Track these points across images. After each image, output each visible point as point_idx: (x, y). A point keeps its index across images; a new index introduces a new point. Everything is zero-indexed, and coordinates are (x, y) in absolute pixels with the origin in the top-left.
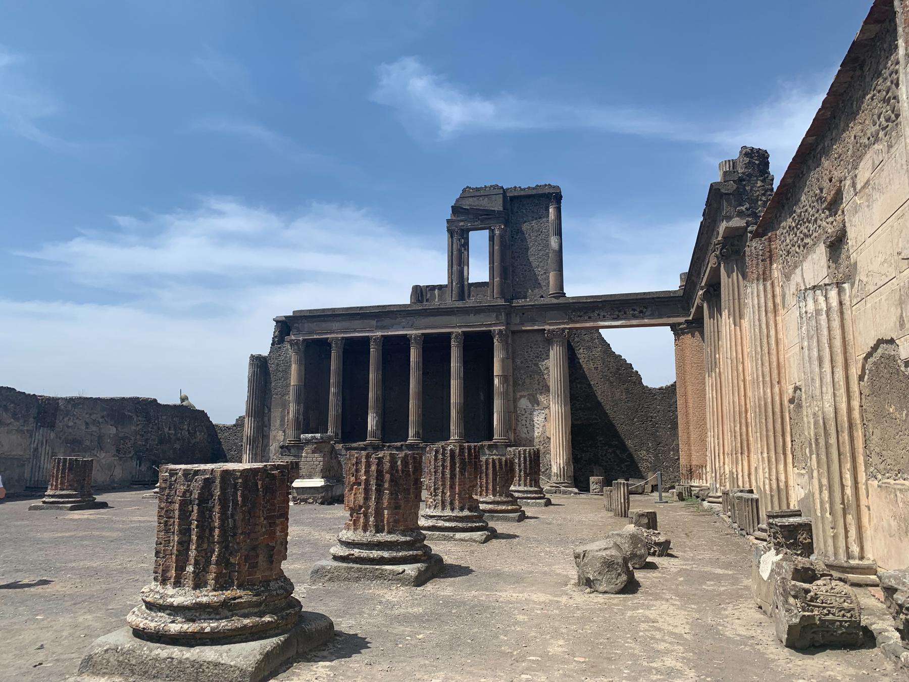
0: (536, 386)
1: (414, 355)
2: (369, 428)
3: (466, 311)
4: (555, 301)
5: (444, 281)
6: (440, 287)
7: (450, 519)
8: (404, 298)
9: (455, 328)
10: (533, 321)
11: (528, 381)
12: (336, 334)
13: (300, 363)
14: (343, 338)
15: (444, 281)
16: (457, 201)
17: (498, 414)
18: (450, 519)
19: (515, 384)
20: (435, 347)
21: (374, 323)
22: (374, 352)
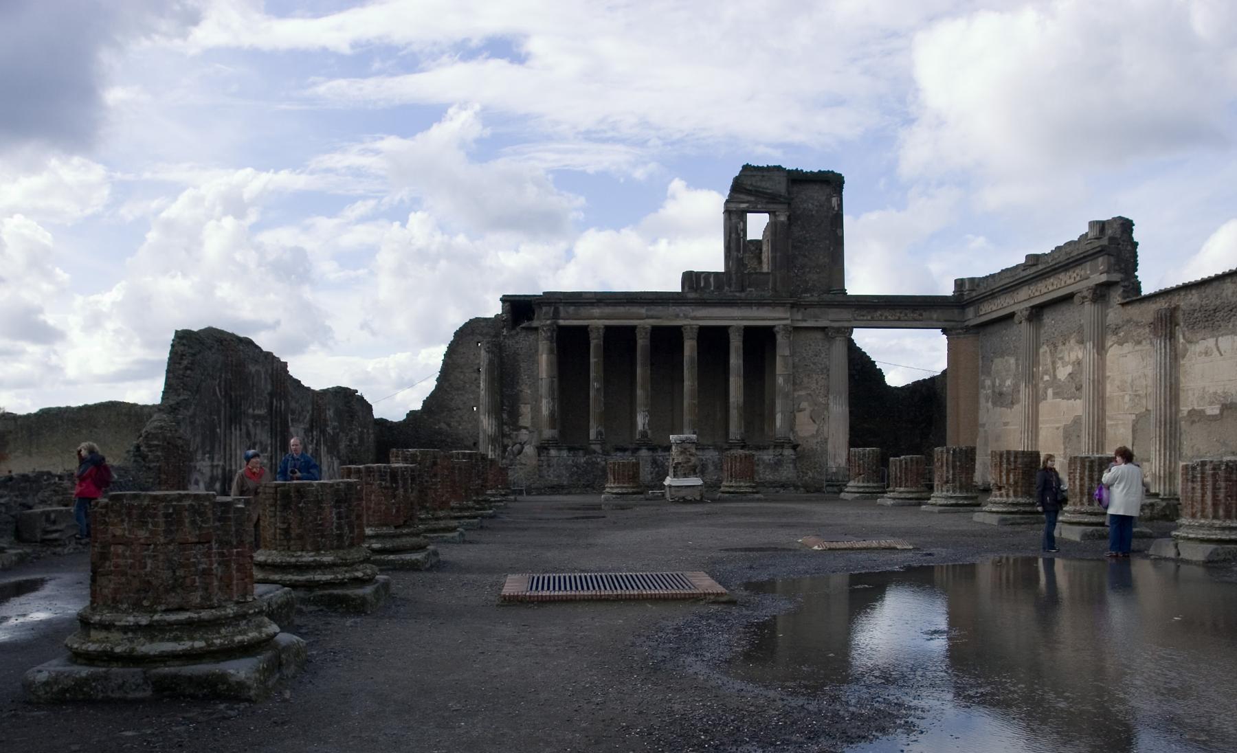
0: (814, 386)
1: (690, 347)
2: (640, 427)
3: (748, 304)
4: (840, 298)
5: (720, 268)
6: (716, 274)
7: (965, 498)
8: (676, 287)
9: (735, 318)
10: (816, 317)
11: (806, 380)
12: (597, 321)
13: (551, 351)
14: (607, 328)
15: (720, 268)
16: (736, 180)
17: (782, 413)
18: (965, 498)
19: (794, 384)
20: (714, 340)
21: (643, 311)
22: (642, 342)
